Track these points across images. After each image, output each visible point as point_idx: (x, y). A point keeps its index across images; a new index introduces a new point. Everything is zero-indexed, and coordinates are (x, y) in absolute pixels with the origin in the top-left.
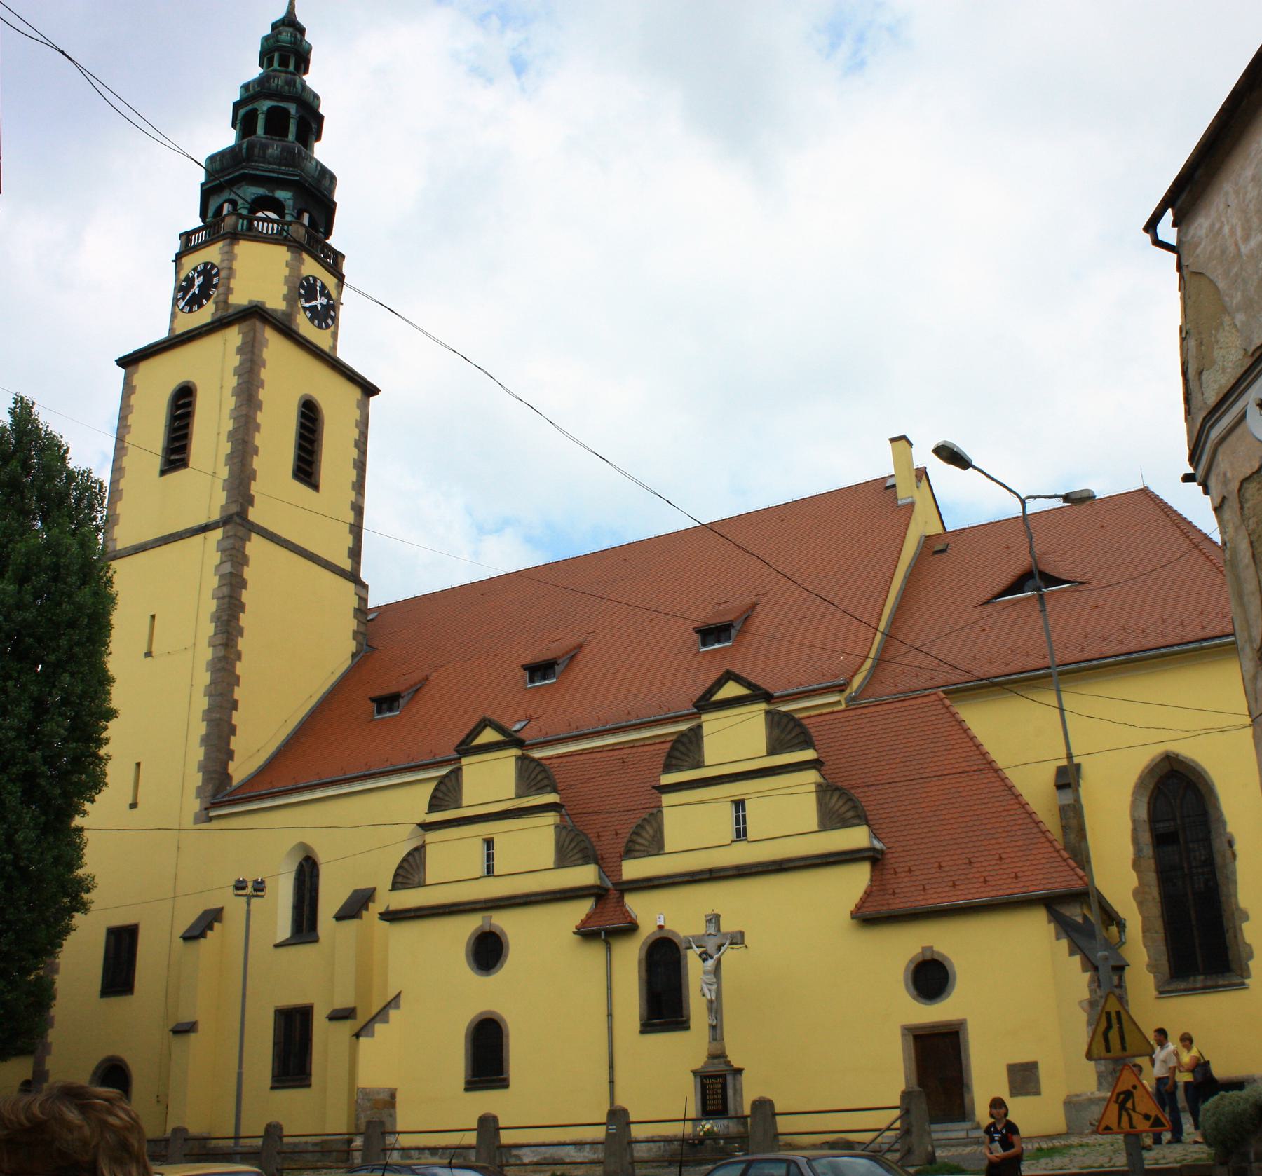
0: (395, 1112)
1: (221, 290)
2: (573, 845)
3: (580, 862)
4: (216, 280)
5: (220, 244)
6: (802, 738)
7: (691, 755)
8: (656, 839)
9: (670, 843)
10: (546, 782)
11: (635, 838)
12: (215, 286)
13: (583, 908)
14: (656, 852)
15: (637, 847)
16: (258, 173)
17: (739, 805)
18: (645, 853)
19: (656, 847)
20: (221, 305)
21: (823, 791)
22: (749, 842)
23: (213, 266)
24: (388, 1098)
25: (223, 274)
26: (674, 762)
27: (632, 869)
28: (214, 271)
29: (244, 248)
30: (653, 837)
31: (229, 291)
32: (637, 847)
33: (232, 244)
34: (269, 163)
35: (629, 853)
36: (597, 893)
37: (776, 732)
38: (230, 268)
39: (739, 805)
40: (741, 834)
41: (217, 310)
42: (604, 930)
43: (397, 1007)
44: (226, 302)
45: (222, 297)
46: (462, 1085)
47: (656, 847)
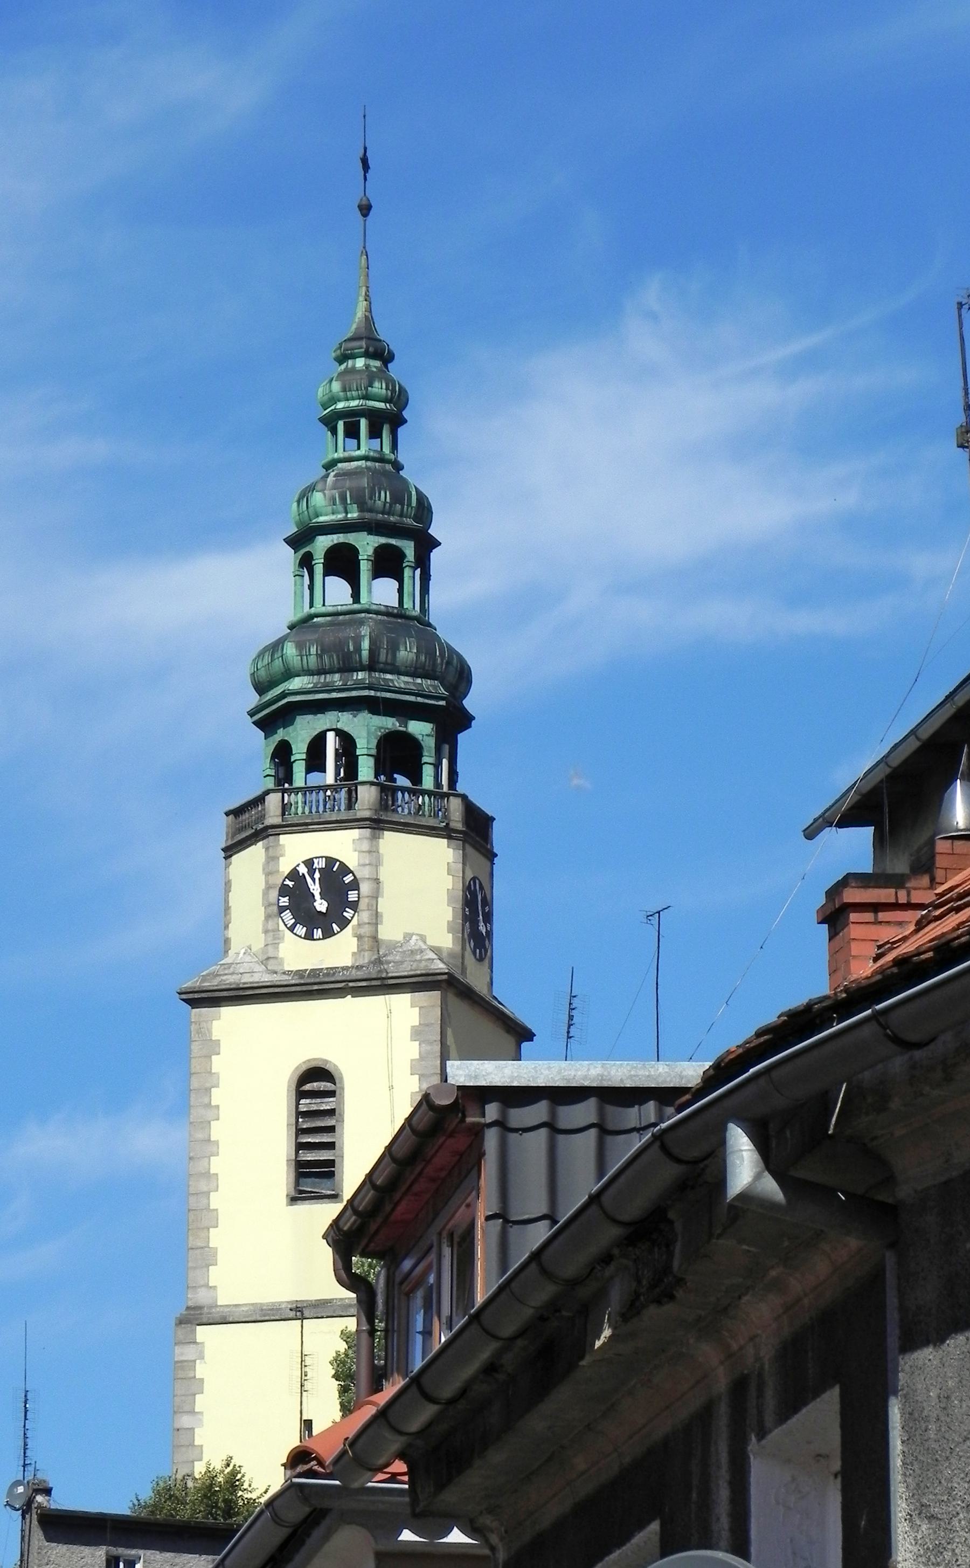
1: (364, 916)
4: (352, 896)
5: (355, 833)
12: (354, 906)
16: (388, 695)
20: (367, 943)
23: (345, 870)
25: (365, 888)
28: (348, 879)
29: (391, 841)
31: (376, 917)
33: (374, 838)
34: (399, 673)
38: (377, 881)
41: (361, 950)
44: (375, 938)
45: (366, 930)
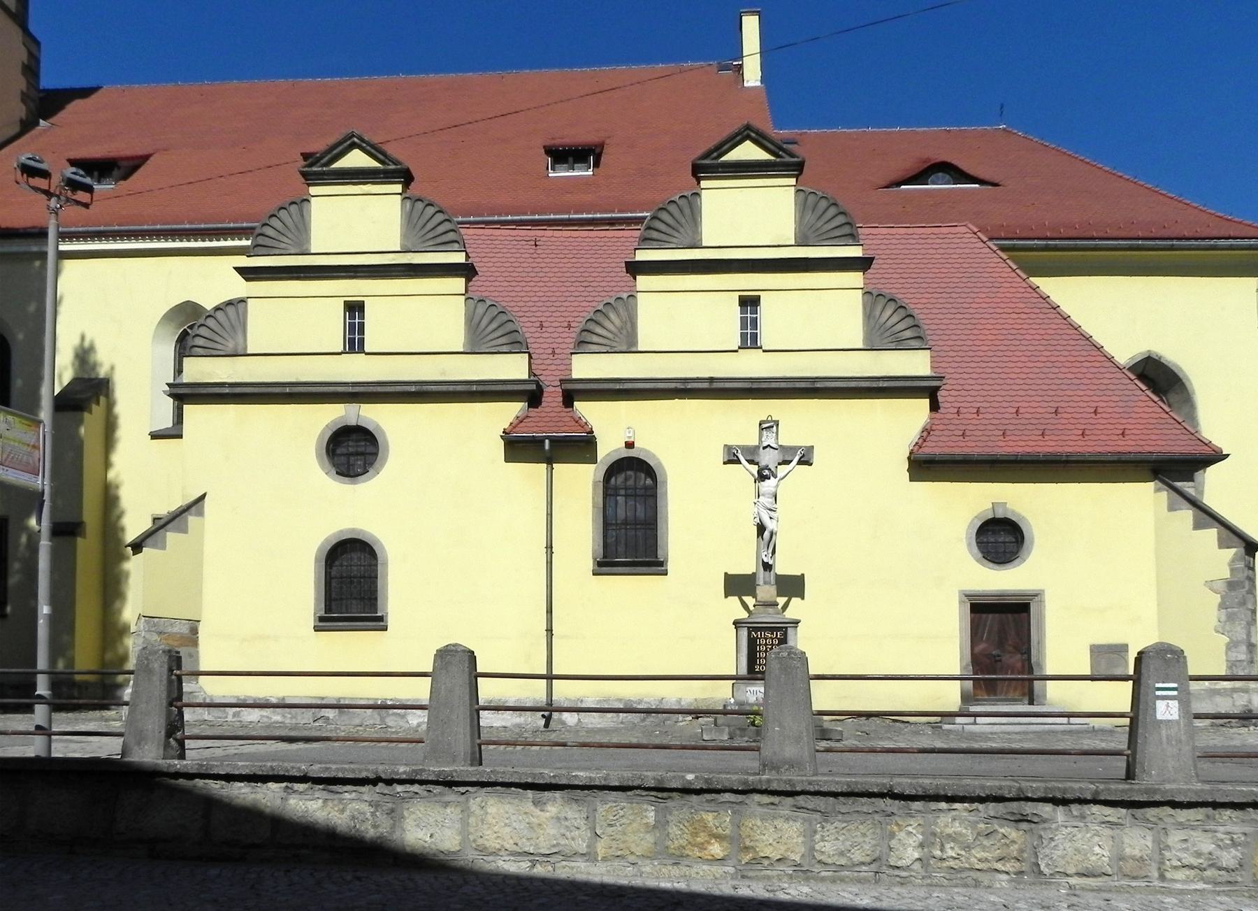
0: (198, 652)
2: (494, 325)
3: (505, 349)
6: (846, 230)
7: (681, 230)
8: (624, 332)
9: (647, 335)
10: (451, 236)
11: (592, 326)
13: (514, 409)
14: (624, 348)
15: (595, 339)
17: (749, 303)
18: (608, 349)
19: (628, 343)
21: (872, 297)
22: (764, 351)
24: (185, 629)
26: (655, 235)
27: (586, 367)
30: (620, 330)
32: (595, 339)
35: (582, 345)
36: (532, 395)
37: (809, 216)
39: (749, 303)
40: (750, 340)
42: (548, 437)
43: (200, 513)
46: (311, 622)
47: (628, 343)
